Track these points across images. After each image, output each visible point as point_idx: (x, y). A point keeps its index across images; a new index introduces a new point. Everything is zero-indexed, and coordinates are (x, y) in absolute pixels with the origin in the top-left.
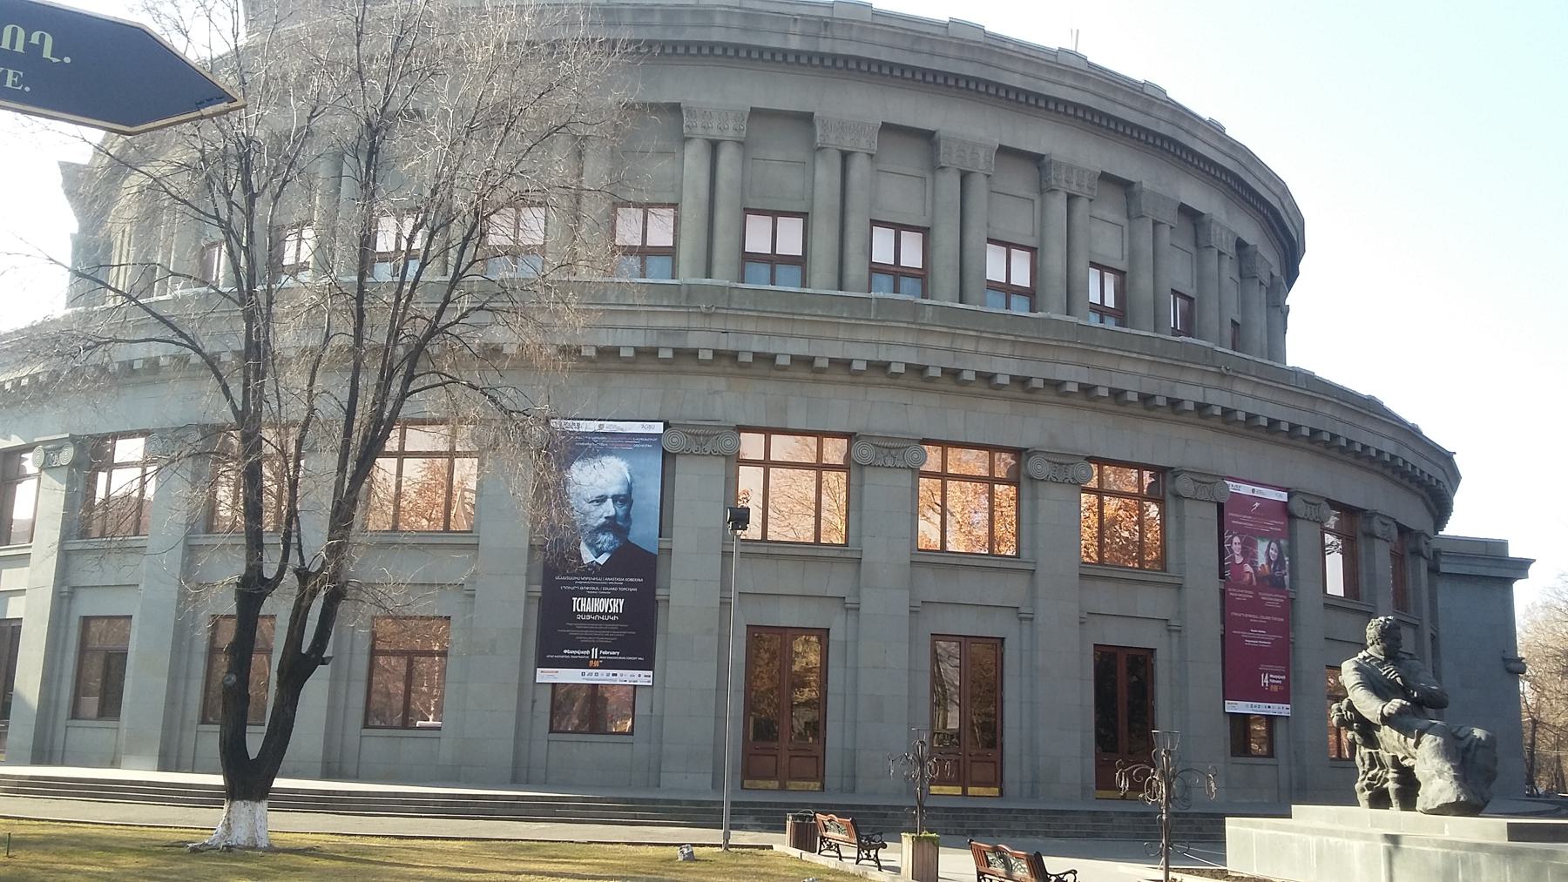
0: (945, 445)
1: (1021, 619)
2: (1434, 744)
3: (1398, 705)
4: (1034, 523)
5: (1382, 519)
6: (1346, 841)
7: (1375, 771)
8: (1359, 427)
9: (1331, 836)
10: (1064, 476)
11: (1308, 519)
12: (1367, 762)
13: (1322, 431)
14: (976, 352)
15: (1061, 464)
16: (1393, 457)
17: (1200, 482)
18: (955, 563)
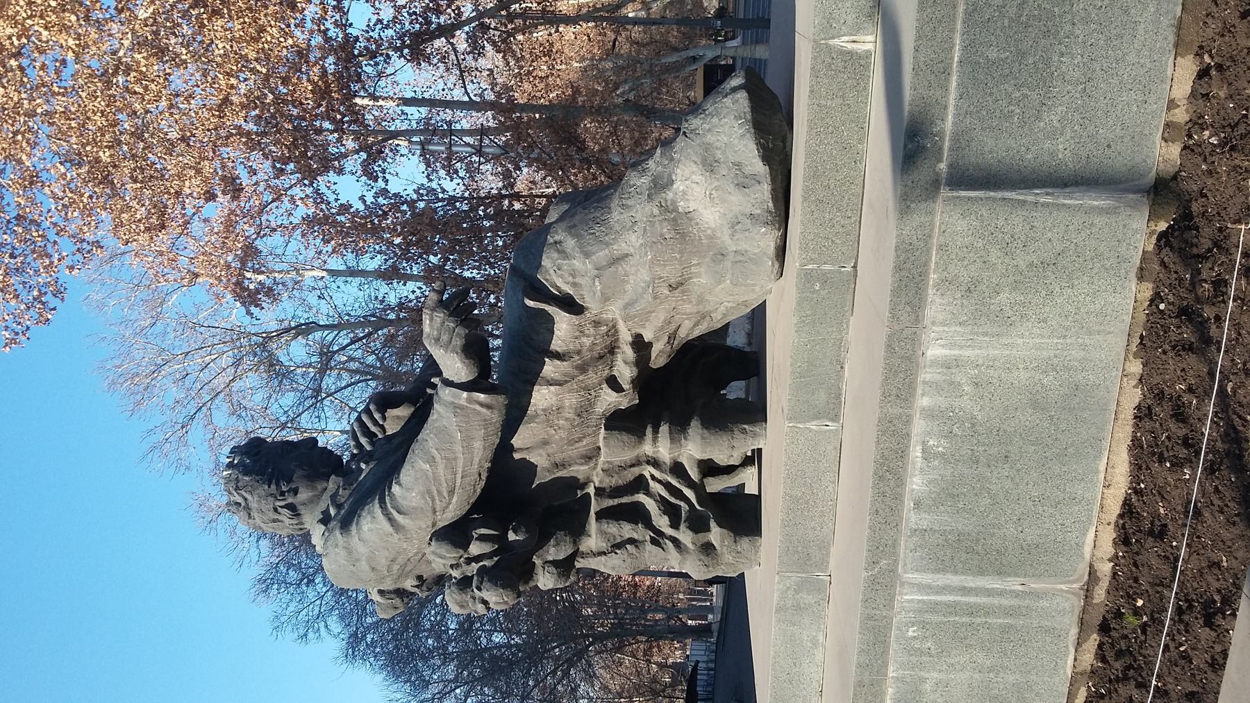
2: (570, 243)
3: (440, 316)
6: (923, 401)
7: (650, 505)
9: (900, 482)
12: (627, 530)
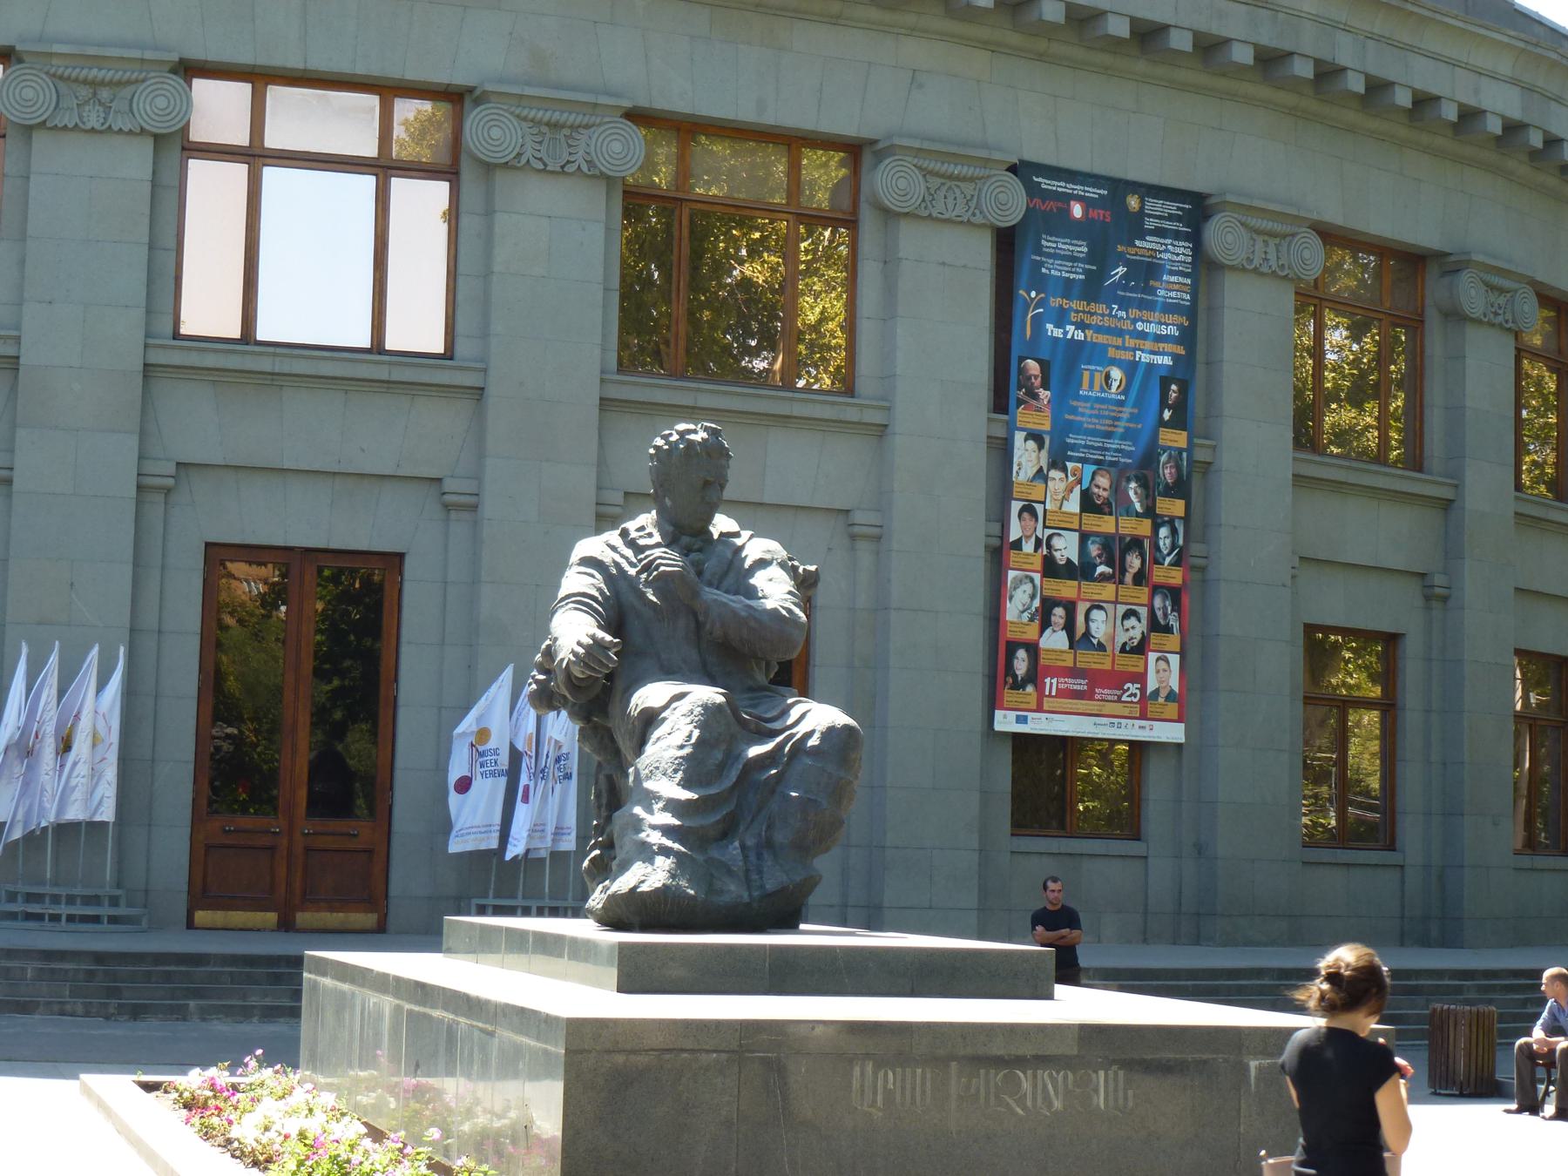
0: (260, 77)
1: (447, 507)
4: (487, 275)
5: (1488, 277)
8: (1411, 49)
10: (566, 157)
11: (1256, 271)
13: (1291, 54)
15: (555, 126)
16: (1513, 129)
17: (942, 176)
18: (268, 369)
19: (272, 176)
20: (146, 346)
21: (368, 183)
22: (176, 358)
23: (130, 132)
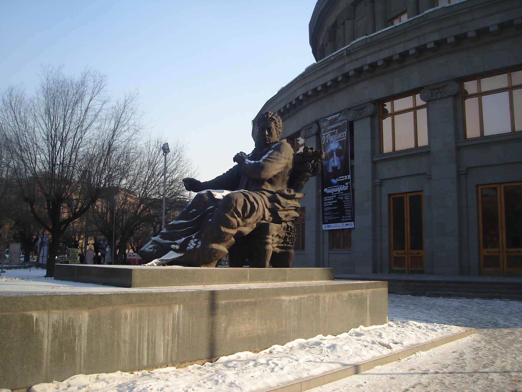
0: (477, 76)
14: (473, 20)
19: (483, 98)
20: (456, 143)
21: (506, 94)
22: (464, 144)
23: (447, 97)
